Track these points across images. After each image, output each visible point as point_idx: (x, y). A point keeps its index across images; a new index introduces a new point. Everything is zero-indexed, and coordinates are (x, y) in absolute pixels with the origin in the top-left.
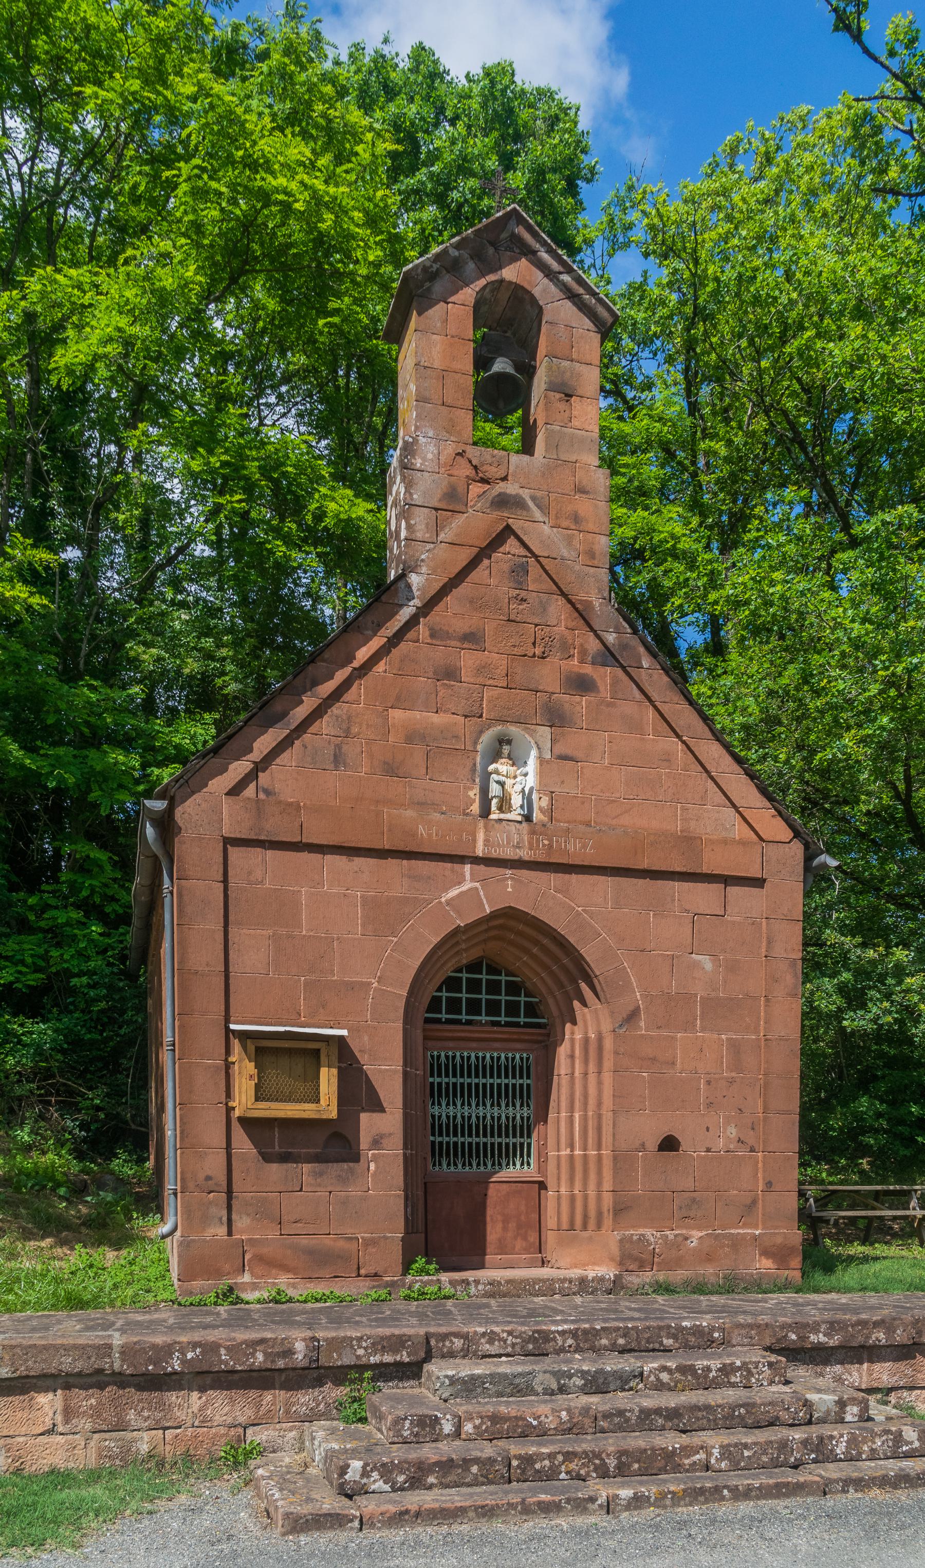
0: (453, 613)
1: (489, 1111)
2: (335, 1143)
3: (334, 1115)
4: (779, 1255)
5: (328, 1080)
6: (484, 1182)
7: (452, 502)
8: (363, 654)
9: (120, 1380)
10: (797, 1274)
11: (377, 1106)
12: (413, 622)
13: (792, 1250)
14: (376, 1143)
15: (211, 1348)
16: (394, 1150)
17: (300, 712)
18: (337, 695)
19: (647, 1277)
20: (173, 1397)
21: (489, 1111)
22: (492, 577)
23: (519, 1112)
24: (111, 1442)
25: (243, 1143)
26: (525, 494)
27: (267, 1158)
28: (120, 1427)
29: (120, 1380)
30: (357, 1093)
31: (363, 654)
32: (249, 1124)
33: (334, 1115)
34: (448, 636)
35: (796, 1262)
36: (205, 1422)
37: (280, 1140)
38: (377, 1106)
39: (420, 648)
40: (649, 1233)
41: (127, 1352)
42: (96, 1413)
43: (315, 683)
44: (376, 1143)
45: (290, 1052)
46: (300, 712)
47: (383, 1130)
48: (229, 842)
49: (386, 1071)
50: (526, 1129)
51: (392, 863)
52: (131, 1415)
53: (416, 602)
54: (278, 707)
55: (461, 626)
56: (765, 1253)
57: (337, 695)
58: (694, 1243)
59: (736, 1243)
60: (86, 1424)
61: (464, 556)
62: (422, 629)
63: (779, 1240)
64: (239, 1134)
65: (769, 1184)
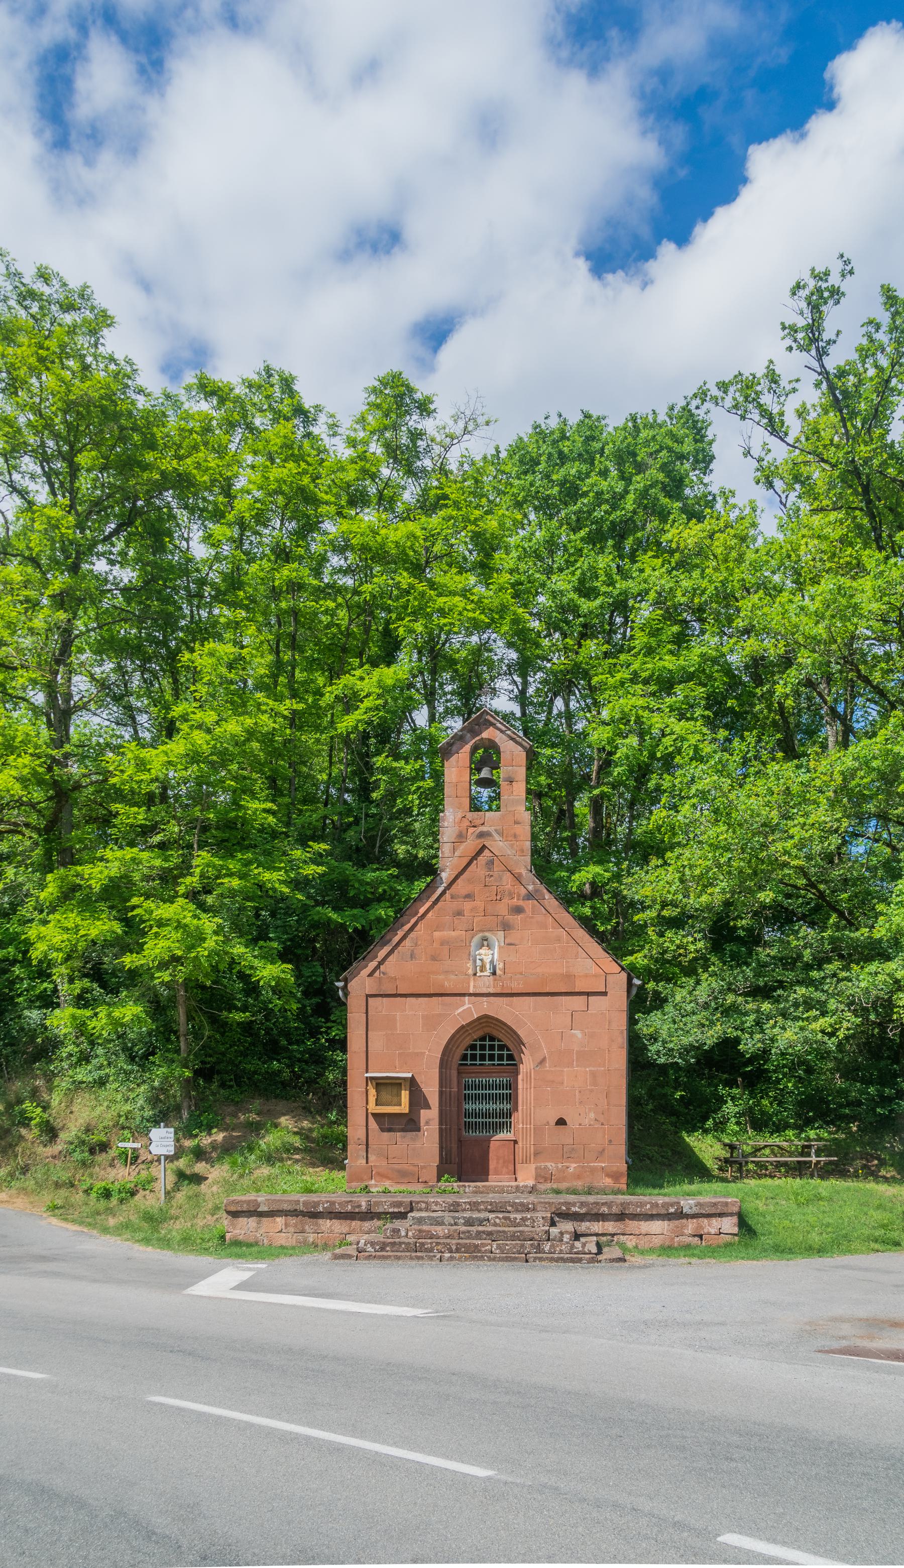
0: (461, 887)
1: (491, 1106)
2: (409, 1123)
3: (407, 1111)
4: (615, 1177)
5: (405, 1095)
6: (488, 1140)
7: (461, 837)
8: (422, 910)
9: (303, 1214)
10: (625, 1186)
11: (428, 1107)
12: (444, 893)
13: (621, 1174)
14: (427, 1123)
15: (333, 1203)
16: (435, 1126)
17: (396, 939)
18: (412, 929)
19: (548, 1185)
20: (321, 1221)
21: (491, 1106)
22: (478, 869)
23: (506, 1106)
24: (300, 1237)
25: (373, 1124)
26: (491, 829)
27: (383, 1130)
28: (303, 1232)
29: (303, 1214)
30: (418, 1100)
31: (422, 910)
32: (374, 1115)
33: (407, 1111)
34: (458, 897)
35: (624, 1180)
36: (332, 1232)
37: (387, 1122)
38: (428, 1107)
39: (447, 903)
40: (549, 1164)
41: (305, 1203)
42: (295, 1226)
43: (403, 925)
44: (427, 1123)
45: (391, 1084)
46: (396, 939)
47: (430, 1117)
48: (368, 996)
49: (431, 1090)
50: (509, 1115)
51: (434, 999)
52: (307, 1227)
53: (445, 885)
54: (388, 938)
55: (464, 892)
56: (608, 1175)
57: (412, 929)
58: (571, 1170)
59: (593, 1170)
60: (292, 1230)
61: (465, 861)
62: (448, 895)
63: (615, 1169)
64: (371, 1118)
65: (610, 1141)
